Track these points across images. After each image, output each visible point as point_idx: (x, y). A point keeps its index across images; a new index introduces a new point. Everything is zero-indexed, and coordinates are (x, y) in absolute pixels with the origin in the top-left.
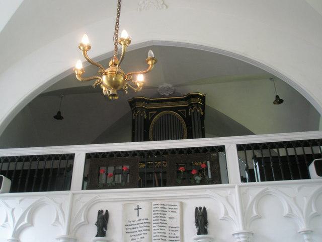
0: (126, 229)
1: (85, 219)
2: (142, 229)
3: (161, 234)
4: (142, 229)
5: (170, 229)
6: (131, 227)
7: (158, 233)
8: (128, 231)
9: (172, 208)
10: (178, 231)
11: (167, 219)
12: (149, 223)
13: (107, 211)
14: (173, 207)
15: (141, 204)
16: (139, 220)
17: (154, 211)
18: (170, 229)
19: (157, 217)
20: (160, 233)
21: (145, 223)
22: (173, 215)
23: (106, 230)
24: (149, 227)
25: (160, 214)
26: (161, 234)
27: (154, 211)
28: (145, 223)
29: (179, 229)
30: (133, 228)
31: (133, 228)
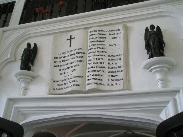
0: (55, 62)
1: (10, 56)
2: (74, 60)
3: (98, 65)
4: (74, 60)
5: (111, 58)
6: (61, 60)
7: (94, 63)
8: (57, 64)
9: (113, 34)
10: (121, 59)
11: (107, 46)
12: (83, 53)
13: (35, 45)
14: (115, 32)
15: (74, 34)
16: (71, 51)
17: (90, 39)
18: (111, 58)
19: (93, 45)
20: (97, 63)
21: (77, 53)
22: (115, 41)
23: (33, 65)
24: (82, 57)
25: (97, 41)
26: (98, 65)
27: (90, 39)
28: (77, 53)
29: (122, 57)
30: (63, 61)
31: (63, 61)
